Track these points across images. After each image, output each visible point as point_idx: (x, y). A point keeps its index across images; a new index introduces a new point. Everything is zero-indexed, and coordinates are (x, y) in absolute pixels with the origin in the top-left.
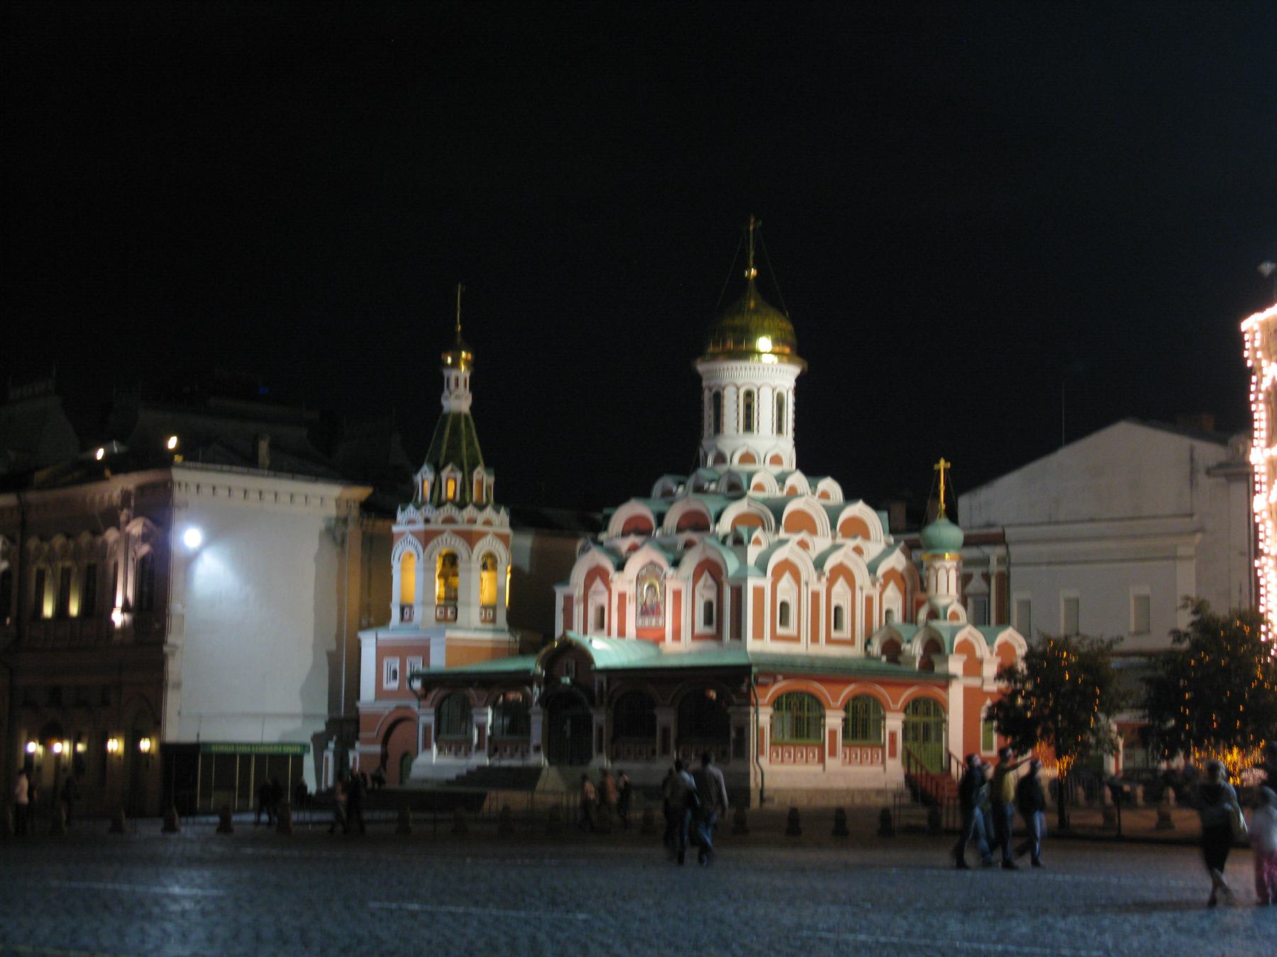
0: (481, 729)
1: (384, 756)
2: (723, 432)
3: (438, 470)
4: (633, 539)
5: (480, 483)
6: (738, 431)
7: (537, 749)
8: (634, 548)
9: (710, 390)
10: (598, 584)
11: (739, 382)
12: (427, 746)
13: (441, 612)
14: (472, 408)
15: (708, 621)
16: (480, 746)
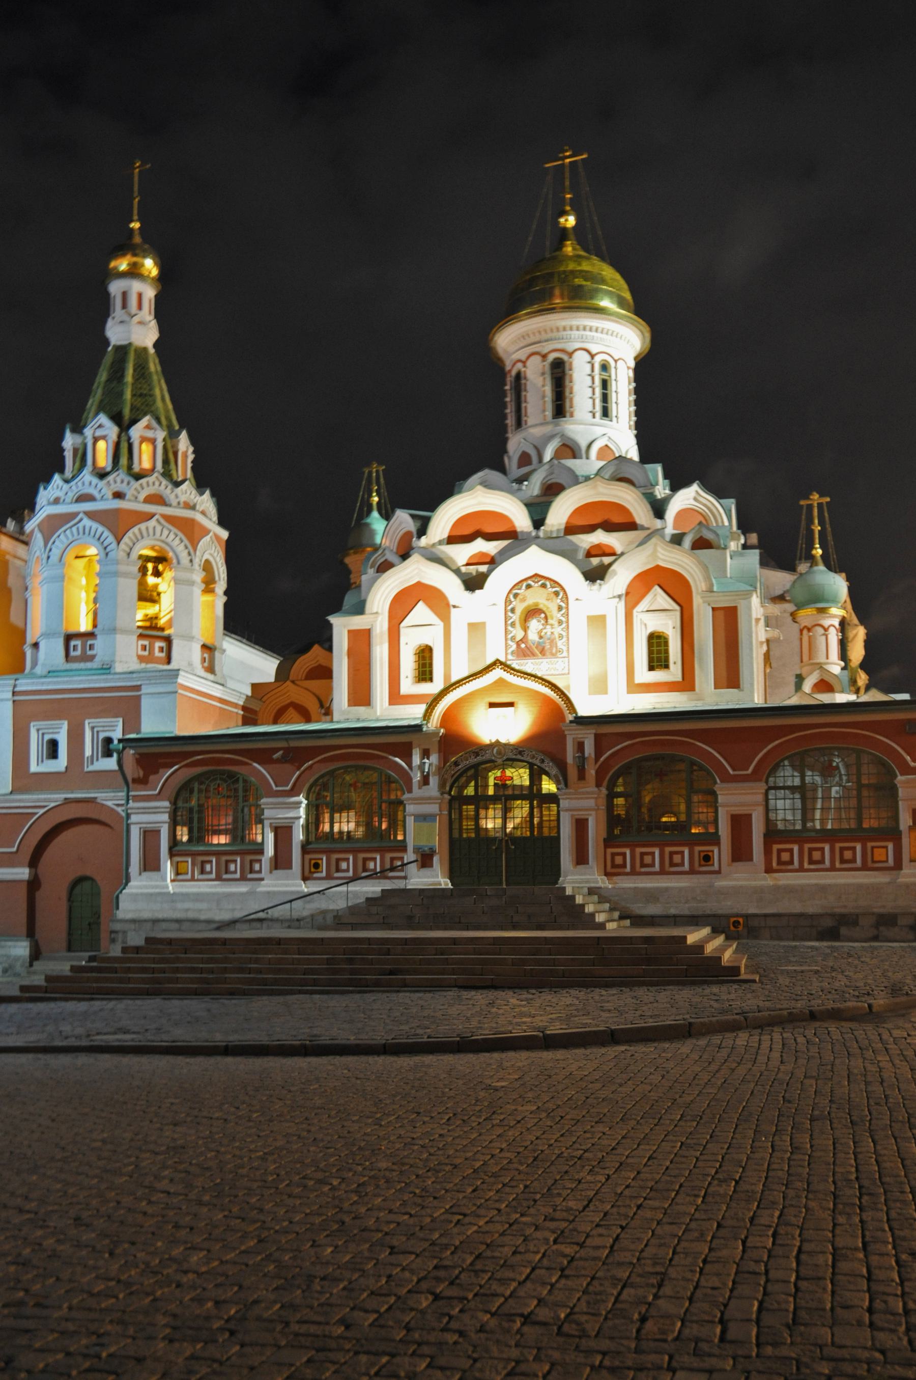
0: (283, 833)
1: (33, 885)
2: (572, 415)
3: (124, 424)
4: (480, 546)
5: (185, 455)
6: (594, 417)
7: (425, 860)
8: (493, 562)
9: (544, 357)
10: (421, 612)
11: (594, 349)
12: (150, 864)
13: (144, 648)
14: (156, 345)
15: (658, 660)
16: (281, 862)
